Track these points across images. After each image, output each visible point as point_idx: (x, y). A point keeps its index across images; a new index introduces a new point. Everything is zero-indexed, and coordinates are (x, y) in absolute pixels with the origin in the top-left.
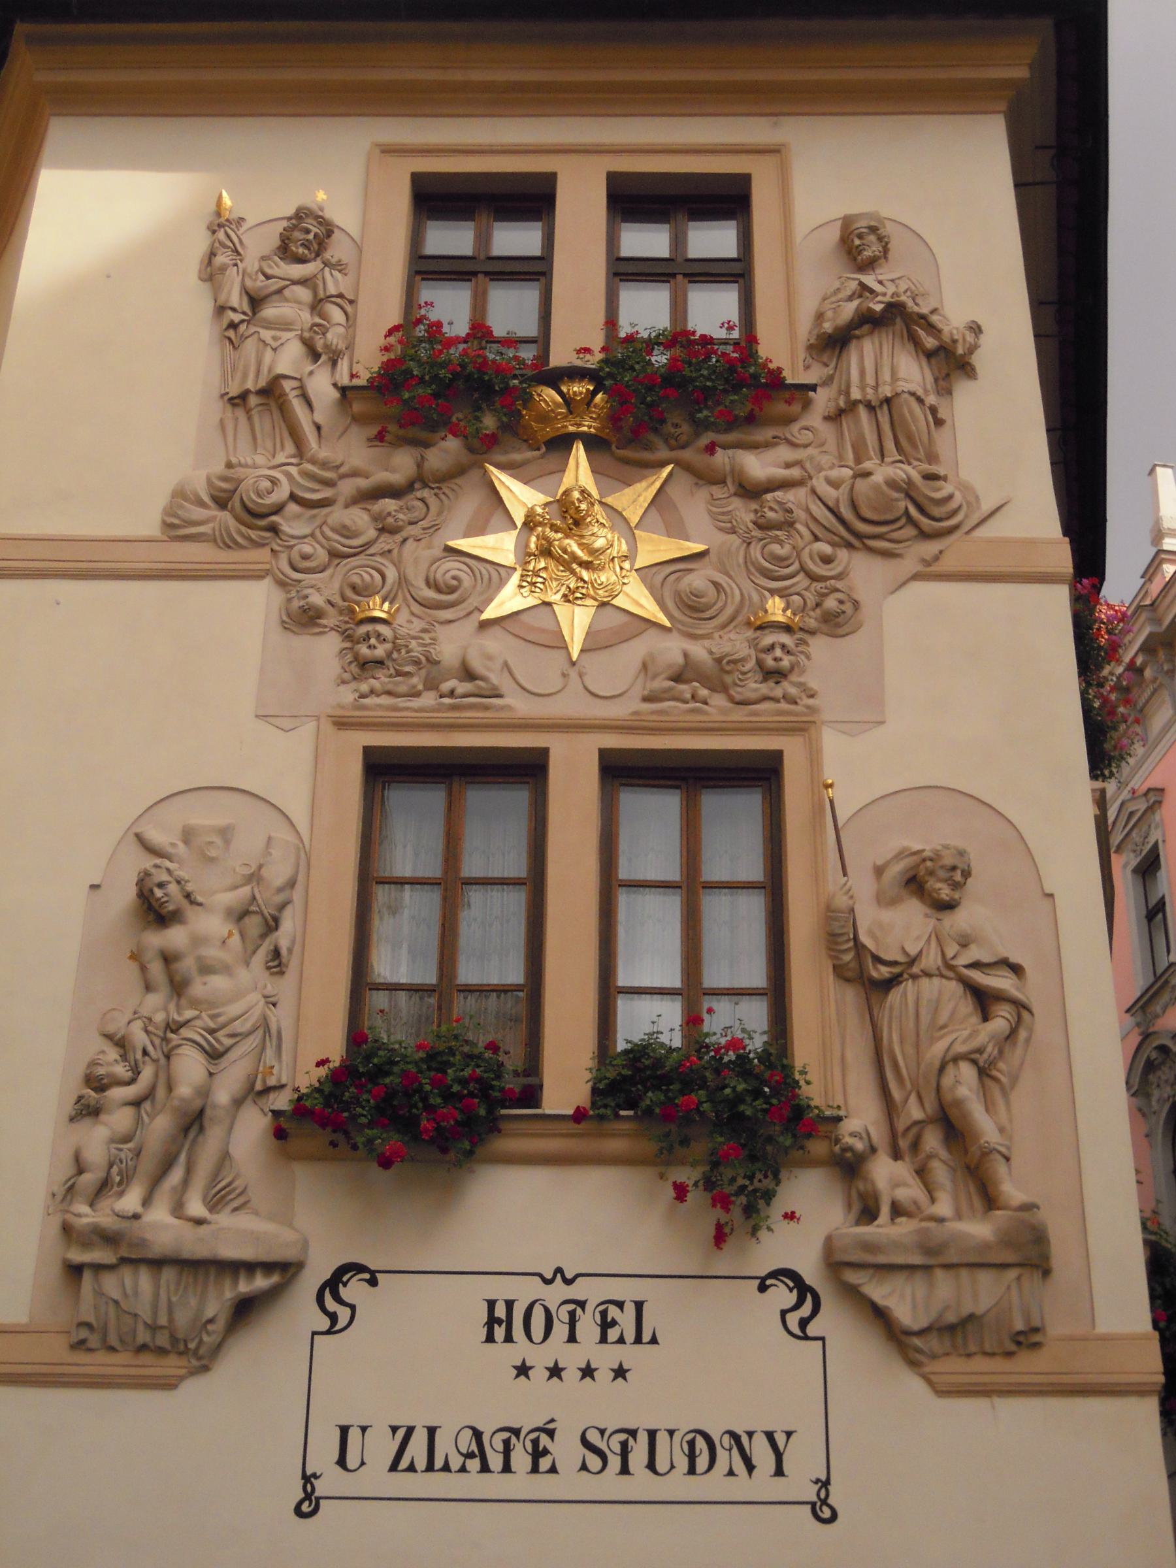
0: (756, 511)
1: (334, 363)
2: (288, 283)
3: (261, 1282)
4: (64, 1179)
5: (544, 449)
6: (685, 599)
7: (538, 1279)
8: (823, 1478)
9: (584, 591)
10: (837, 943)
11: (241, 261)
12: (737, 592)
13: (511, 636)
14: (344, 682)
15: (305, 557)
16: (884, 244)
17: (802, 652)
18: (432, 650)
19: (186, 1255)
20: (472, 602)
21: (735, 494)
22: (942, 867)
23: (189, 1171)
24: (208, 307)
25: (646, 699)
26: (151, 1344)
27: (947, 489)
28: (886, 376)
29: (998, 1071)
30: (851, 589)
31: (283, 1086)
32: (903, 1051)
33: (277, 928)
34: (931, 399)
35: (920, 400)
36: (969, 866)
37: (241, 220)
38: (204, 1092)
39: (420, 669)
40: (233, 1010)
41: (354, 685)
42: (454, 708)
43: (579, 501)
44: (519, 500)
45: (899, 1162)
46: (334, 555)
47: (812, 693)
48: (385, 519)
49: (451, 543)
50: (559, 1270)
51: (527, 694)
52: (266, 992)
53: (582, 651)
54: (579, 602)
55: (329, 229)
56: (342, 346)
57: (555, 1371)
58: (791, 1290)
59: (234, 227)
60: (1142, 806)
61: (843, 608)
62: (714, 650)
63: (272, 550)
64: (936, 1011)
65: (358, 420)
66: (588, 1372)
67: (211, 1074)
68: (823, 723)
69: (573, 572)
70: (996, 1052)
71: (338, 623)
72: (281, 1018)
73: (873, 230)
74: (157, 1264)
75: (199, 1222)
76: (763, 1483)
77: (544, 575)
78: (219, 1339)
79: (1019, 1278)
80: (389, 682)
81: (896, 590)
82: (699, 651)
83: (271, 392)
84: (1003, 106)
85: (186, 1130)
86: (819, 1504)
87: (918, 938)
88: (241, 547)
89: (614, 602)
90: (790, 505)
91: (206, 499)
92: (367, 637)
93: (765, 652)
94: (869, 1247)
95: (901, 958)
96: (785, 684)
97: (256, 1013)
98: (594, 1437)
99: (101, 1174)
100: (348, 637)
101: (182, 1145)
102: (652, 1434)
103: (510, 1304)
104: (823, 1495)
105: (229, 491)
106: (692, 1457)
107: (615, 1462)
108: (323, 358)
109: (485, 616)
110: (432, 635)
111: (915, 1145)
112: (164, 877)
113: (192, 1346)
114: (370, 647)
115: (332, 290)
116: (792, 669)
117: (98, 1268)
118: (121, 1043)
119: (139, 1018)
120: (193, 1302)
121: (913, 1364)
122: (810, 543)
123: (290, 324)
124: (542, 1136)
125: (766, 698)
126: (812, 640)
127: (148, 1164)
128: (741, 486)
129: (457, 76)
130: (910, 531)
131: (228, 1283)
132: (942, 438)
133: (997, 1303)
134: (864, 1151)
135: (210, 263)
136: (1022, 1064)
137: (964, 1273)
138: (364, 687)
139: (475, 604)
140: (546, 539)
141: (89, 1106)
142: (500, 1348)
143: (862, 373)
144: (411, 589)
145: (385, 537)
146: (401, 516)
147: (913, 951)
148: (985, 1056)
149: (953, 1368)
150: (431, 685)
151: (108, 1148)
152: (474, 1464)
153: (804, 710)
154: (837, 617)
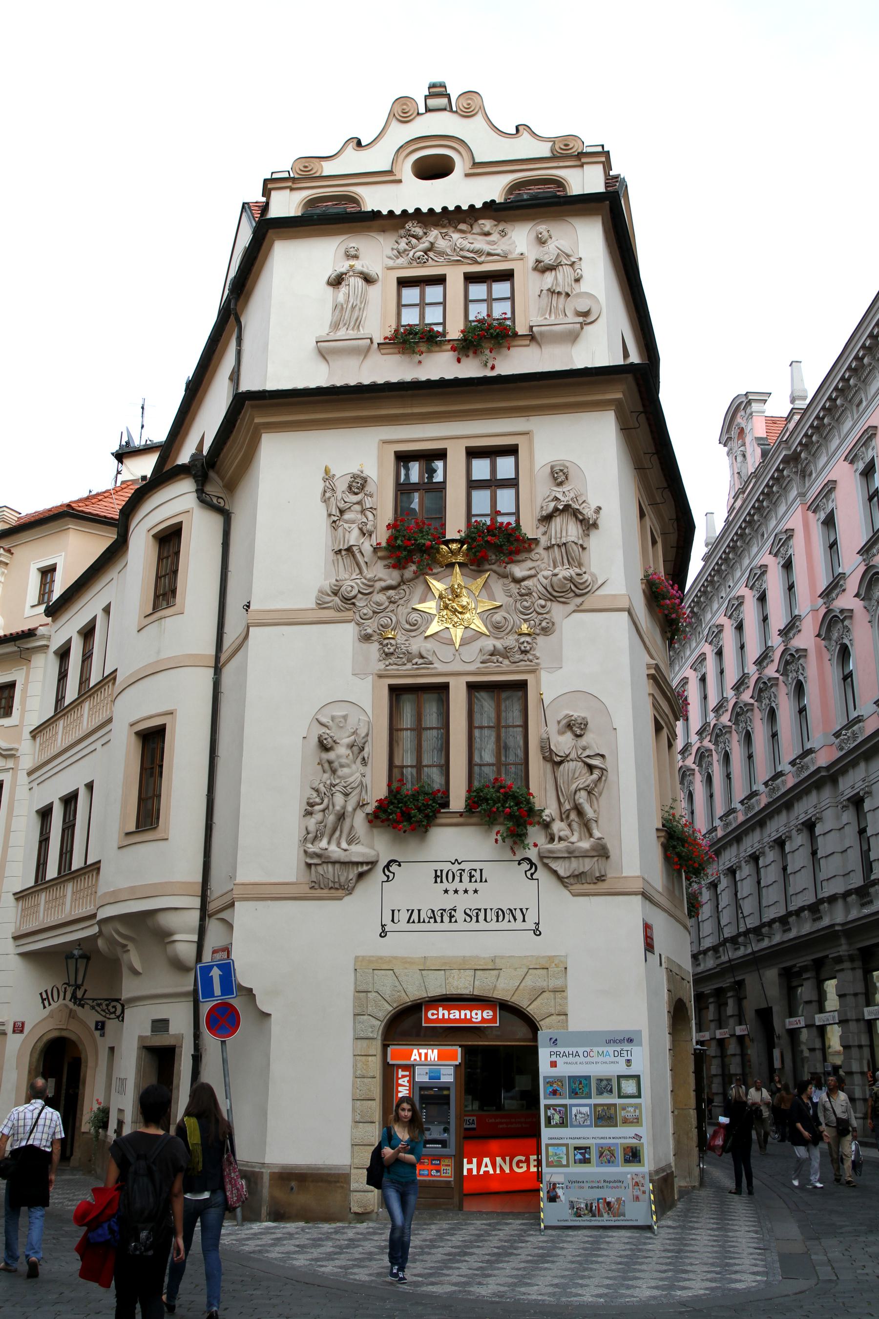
0: (519, 589)
1: (371, 535)
3: (365, 868)
15: (365, 615)
19: (342, 861)
20: (422, 629)
23: (341, 832)
24: (325, 514)
25: (482, 663)
28: (564, 534)
30: (551, 617)
33: (363, 750)
34: (580, 542)
35: (576, 544)
37: (334, 475)
38: (344, 807)
40: (351, 779)
41: (384, 661)
46: (374, 612)
50: (456, 860)
55: (365, 480)
57: (456, 891)
60: (784, 537)
64: (574, 773)
65: (380, 558)
66: (466, 891)
69: (456, 615)
72: (367, 780)
73: (561, 470)
74: (334, 863)
75: (346, 850)
76: (519, 924)
82: (499, 644)
83: (349, 550)
84: (614, 408)
85: (339, 819)
91: (330, 593)
92: (387, 644)
94: (550, 851)
96: (528, 655)
97: (359, 779)
98: (468, 911)
99: (315, 834)
100: (381, 644)
102: (486, 910)
103: (441, 871)
106: (498, 917)
107: (474, 919)
109: (426, 635)
110: (408, 642)
111: (568, 817)
112: (327, 736)
115: (368, 506)
116: (531, 649)
117: (316, 865)
118: (317, 791)
120: (345, 874)
121: (565, 887)
125: (522, 660)
126: (537, 637)
127: (328, 831)
129: (408, 411)
130: (572, 594)
132: (584, 556)
137: (580, 859)
138: (387, 663)
142: (439, 884)
145: (391, 605)
146: (397, 597)
147: (567, 753)
149: (577, 888)
150: (409, 661)
152: (432, 920)
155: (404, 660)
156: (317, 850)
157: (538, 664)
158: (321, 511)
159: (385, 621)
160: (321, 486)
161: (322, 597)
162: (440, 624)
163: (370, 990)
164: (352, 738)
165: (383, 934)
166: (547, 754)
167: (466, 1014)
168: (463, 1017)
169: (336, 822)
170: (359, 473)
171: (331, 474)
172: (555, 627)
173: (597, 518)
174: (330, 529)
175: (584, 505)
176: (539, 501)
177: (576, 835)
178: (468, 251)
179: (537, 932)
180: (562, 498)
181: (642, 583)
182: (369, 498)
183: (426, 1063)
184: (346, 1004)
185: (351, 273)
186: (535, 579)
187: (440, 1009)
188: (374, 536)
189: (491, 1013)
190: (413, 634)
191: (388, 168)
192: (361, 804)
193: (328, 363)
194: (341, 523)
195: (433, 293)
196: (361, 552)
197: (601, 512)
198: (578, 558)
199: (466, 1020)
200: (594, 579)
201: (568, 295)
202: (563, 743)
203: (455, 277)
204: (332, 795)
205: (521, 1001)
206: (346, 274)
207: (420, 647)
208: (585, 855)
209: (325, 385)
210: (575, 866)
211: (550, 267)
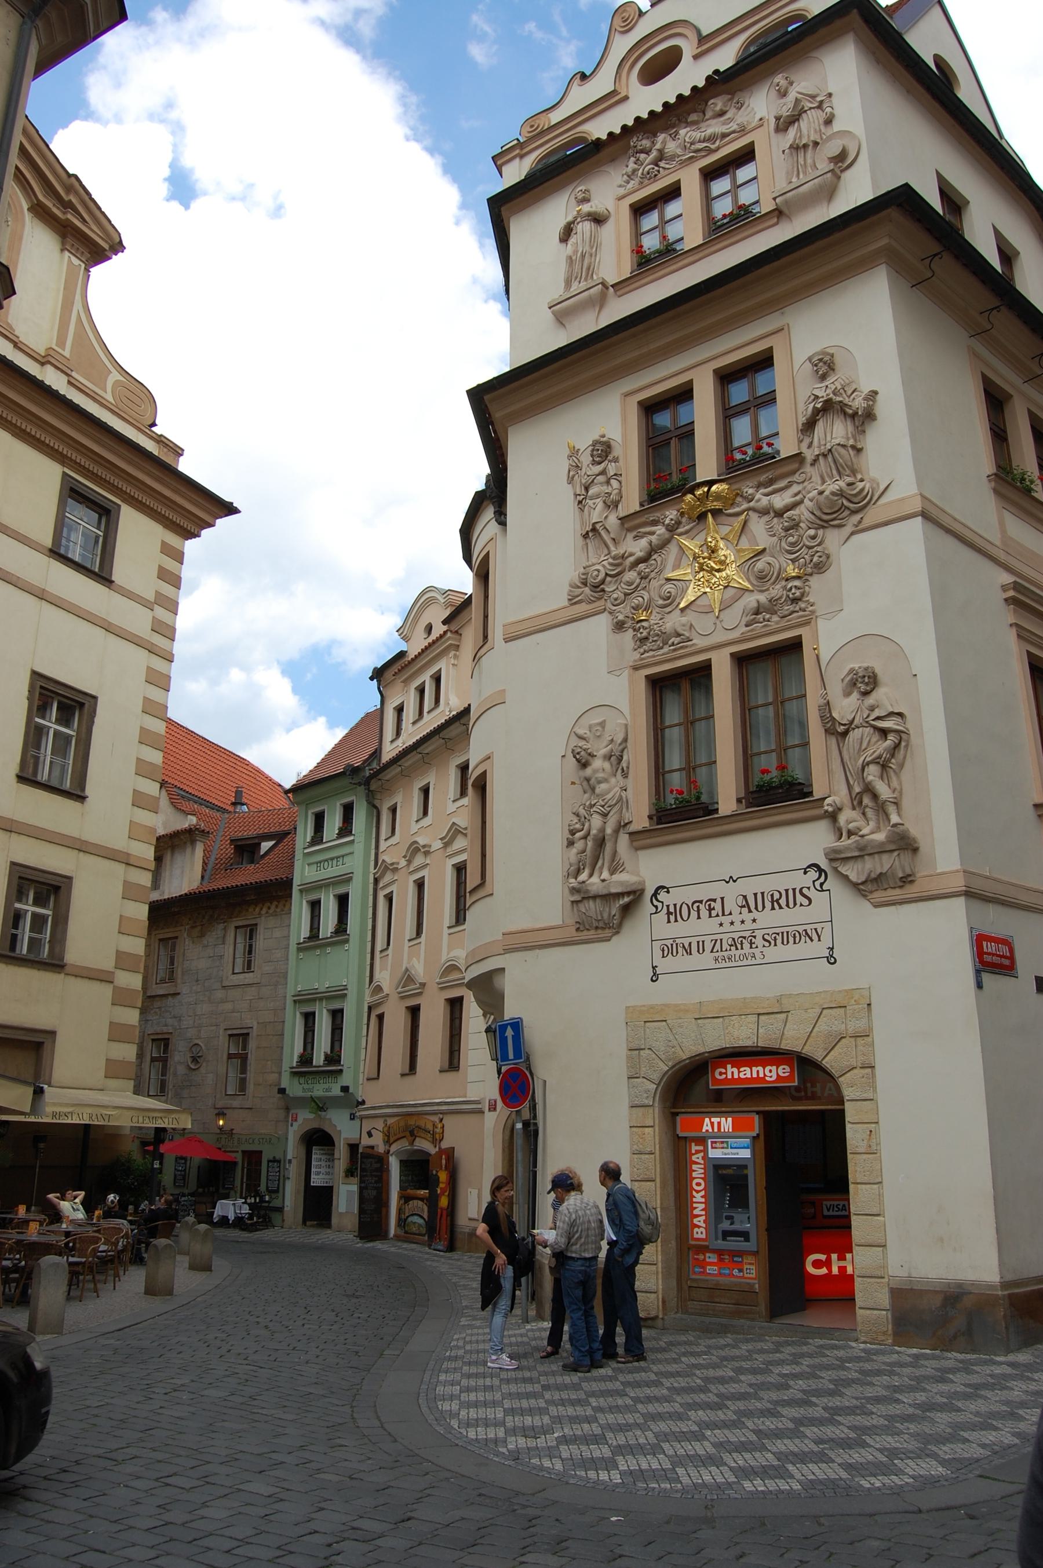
1: (617, 506)
3: (626, 899)
12: (777, 566)
15: (616, 599)
20: (677, 600)
21: (775, 517)
24: (572, 496)
25: (747, 626)
27: (860, 485)
28: (829, 438)
34: (851, 442)
35: (844, 446)
36: (873, 673)
38: (602, 830)
42: (675, 650)
46: (626, 595)
50: (731, 877)
53: (720, 611)
61: (821, 559)
68: (817, 617)
72: (630, 794)
73: (821, 360)
74: (594, 897)
75: (603, 881)
82: (763, 598)
83: (594, 529)
88: (595, 601)
92: (640, 628)
94: (835, 851)
96: (800, 603)
99: (576, 867)
100: (634, 630)
111: (860, 802)
112: (579, 750)
116: (803, 595)
118: (577, 815)
120: (607, 910)
121: (865, 896)
124: (717, 826)
127: (588, 861)
128: (775, 512)
129: (645, 350)
130: (847, 512)
136: (905, 758)
137: (876, 856)
138: (642, 650)
146: (647, 570)
147: (850, 718)
149: (879, 896)
150: (665, 643)
160: (565, 464)
161: (571, 591)
162: (696, 590)
163: (643, 1047)
166: (829, 725)
167: (758, 1071)
168: (755, 1075)
172: (830, 559)
175: (855, 394)
176: (801, 407)
177: (872, 824)
178: (700, 141)
179: (831, 960)
181: (990, 481)
182: (613, 464)
183: (719, 1134)
184: (619, 1065)
185: (579, 220)
186: (802, 506)
187: (729, 1066)
189: (788, 1069)
191: (613, 89)
192: (622, 824)
193: (564, 325)
195: (672, 209)
196: (605, 528)
197: (879, 397)
199: (758, 1079)
200: (875, 485)
201: (816, 144)
202: (845, 708)
203: (690, 180)
205: (814, 1051)
206: (573, 222)
208: (881, 850)
210: (871, 866)
211: (792, 119)
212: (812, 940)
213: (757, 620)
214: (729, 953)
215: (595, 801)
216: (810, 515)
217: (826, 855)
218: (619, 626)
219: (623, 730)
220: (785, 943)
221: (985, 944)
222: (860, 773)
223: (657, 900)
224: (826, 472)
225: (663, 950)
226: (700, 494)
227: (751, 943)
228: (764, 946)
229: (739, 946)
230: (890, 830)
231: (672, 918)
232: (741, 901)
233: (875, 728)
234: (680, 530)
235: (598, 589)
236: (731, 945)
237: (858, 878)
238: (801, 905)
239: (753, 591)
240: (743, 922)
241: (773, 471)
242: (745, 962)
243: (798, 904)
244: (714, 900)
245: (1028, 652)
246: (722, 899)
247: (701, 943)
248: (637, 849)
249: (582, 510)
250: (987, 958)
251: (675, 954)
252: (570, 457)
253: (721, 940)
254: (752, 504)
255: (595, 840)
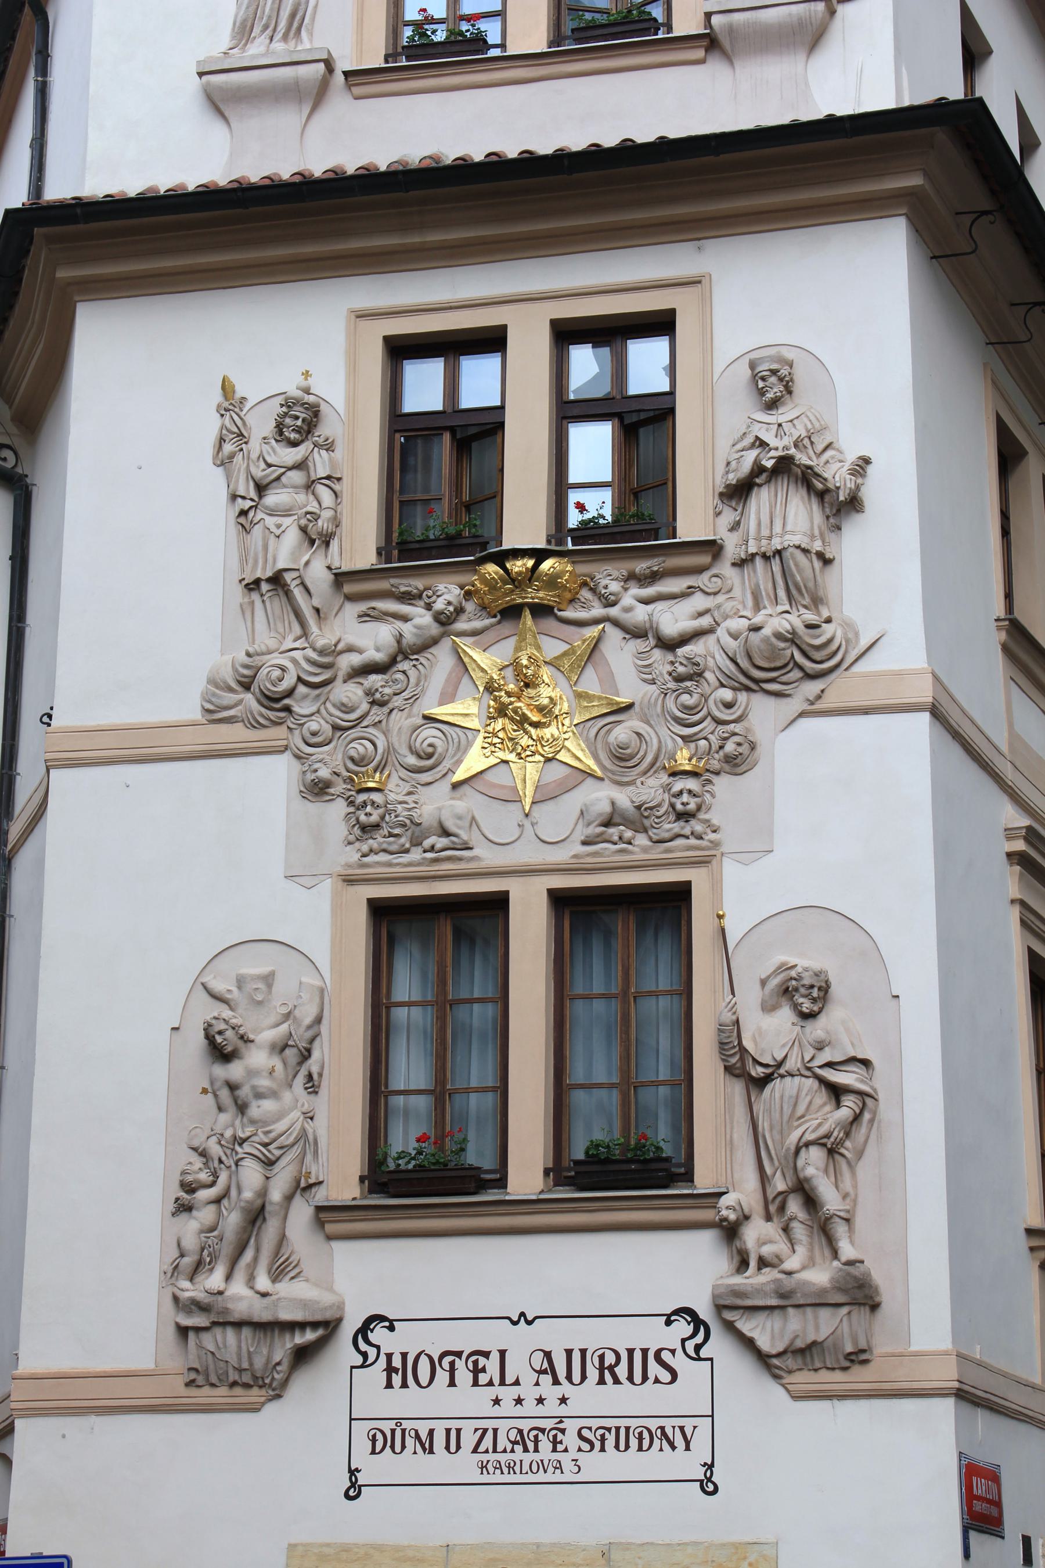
0: (672, 663)
1: (327, 544)
2: (283, 470)
3: (310, 1336)
4: (171, 1261)
5: (499, 617)
6: (613, 751)
7: (507, 1321)
8: (709, 1463)
9: (533, 749)
10: (724, 1050)
11: (246, 443)
12: (655, 741)
13: (477, 793)
14: (350, 843)
15: (314, 734)
16: (784, 383)
17: (707, 791)
18: (414, 814)
19: (256, 1319)
20: (446, 764)
21: (656, 646)
22: (803, 986)
23: (258, 1250)
25: (585, 843)
26: (240, 1382)
28: (778, 528)
29: (846, 1149)
30: (748, 730)
31: (321, 1183)
32: (772, 1136)
33: (310, 1056)
34: (817, 546)
35: (806, 551)
36: (827, 982)
38: (263, 1193)
39: (406, 830)
40: (280, 1127)
41: (357, 844)
42: (436, 861)
43: (527, 667)
44: (479, 666)
45: (769, 1223)
46: (336, 728)
47: (715, 828)
48: (374, 694)
49: (425, 712)
51: (491, 844)
52: (304, 1109)
53: (533, 803)
54: (530, 759)
56: (331, 528)
58: (689, 1323)
59: (236, 410)
61: (740, 750)
62: (634, 800)
63: (288, 727)
64: (795, 1104)
67: (268, 1178)
68: (722, 854)
69: (526, 732)
70: (841, 1135)
71: (343, 791)
72: (320, 1127)
73: (774, 372)
74: (238, 1325)
75: (264, 1295)
77: (501, 735)
78: (286, 1376)
79: (849, 1313)
80: (384, 842)
81: (786, 727)
82: (624, 798)
83: (277, 580)
85: (253, 1222)
86: (705, 1481)
87: (784, 1046)
89: (557, 757)
90: (698, 659)
91: (234, 685)
92: (364, 804)
93: (675, 797)
94: (737, 1293)
95: (772, 1063)
96: (693, 822)
97: (298, 1126)
99: (196, 1257)
100: (351, 803)
101: (252, 1232)
104: (708, 1475)
105: (251, 677)
108: (317, 541)
111: (782, 1208)
112: (222, 1026)
113: (267, 1381)
114: (366, 814)
115: (322, 473)
116: (699, 808)
117: (198, 1330)
118: (203, 1154)
119: (215, 1135)
120: (265, 1351)
121: (776, 1377)
122: (716, 689)
123: (289, 510)
125: (679, 836)
127: (226, 1250)
130: (796, 674)
131: (288, 1336)
132: (830, 580)
133: (832, 1333)
134: (738, 1219)
135: (220, 447)
137: (809, 1310)
138: (365, 848)
139: (448, 766)
140: (503, 704)
141: (183, 1205)
143: (759, 524)
144: (398, 756)
145: (375, 709)
147: (779, 1058)
148: (832, 1139)
149: (803, 1379)
150: (416, 842)
151: (200, 1238)
153: (708, 844)
154: (735, 759)
155: (403, 840)
156: (201, 1296)
157: (716, 844)
158: (216, 482)
159: (359, 748)
160: (212, 425)
161: (214, 695)
164: (284, 1028)
165: (353, 1491)
166: (733, 1060)
169: (244, 1229)
170: (299, 394)
171: (239, 395)
173: (858, 488)
174: (233, 529)
175: (829, 453)
176: (724, 450)
177: (801, 1250)
179: (708, 1486)
180: (772, 442)
181: (999, 628)
182: (323, 453)
186: (711, 639)
188: (334, 544)
190: (425, 777)
194: (260, 515)
196: (303, 584)
197: (870, 470)
198: (811, 585)
200: (850, 635)
204: (237, 1165)
207: (439, 809)
209: (223, 182)
212: (673, 1448)
213: (605, 837)
214: (509, 1456)
215: (248, 1134)
216: (728, 662)
217: (715, 1297)
218: (318, 789)
219: (317, 1000)
220: (622, 1447)
221: (974, 1479)
222: (791, 1160)
223: (368, 1342)
224: (766, 591)
225: (374, 1440)
226: (519, 573)
227: (555, 1442)
228: (580, 1450)
229: (531, 1446)
230: (841, 1270)
231: (397, 1379)
232: (538, 1360)
233: (823, 1081)
234: (461, 625)
235: (278, 706)
236: (515, 1443)
237: (773, 1345)
238: (657, 1381)
239: (601, 779)
240: (540, 1401)
241: (661, 559)
242: (541, 1477)
243: (652, 1379)
244: (486, 1355)
245: (1029, 948)
246: (502, 1353)
247: (453, 1434)
248: (330, 1238)
249: (246, 530)
250: (978, 1506)
251: (398, 1448)
252: (223, 411)
253: (495, 1431)
254: (614, 612)
255: (246, 1211)
